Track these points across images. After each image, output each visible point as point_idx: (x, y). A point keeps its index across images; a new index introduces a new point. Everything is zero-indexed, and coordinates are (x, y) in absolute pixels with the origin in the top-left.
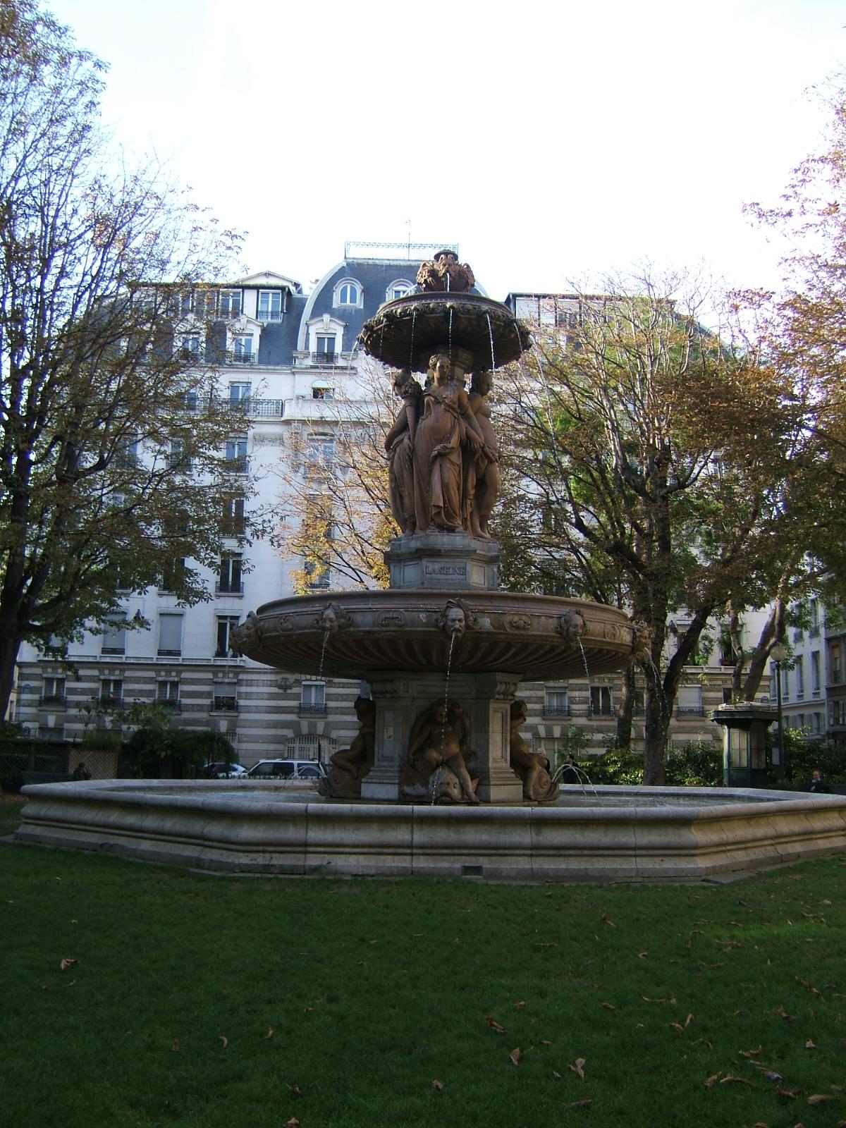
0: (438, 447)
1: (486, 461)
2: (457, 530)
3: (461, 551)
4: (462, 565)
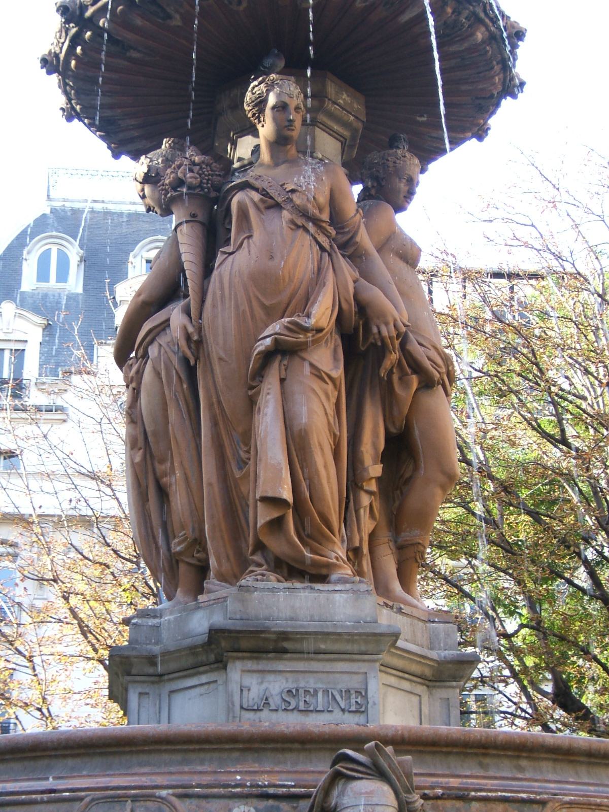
0: (276, 327)
1: (414, 381)
2: (334, 577)
3: (351, 637)
4: (354, 682)
